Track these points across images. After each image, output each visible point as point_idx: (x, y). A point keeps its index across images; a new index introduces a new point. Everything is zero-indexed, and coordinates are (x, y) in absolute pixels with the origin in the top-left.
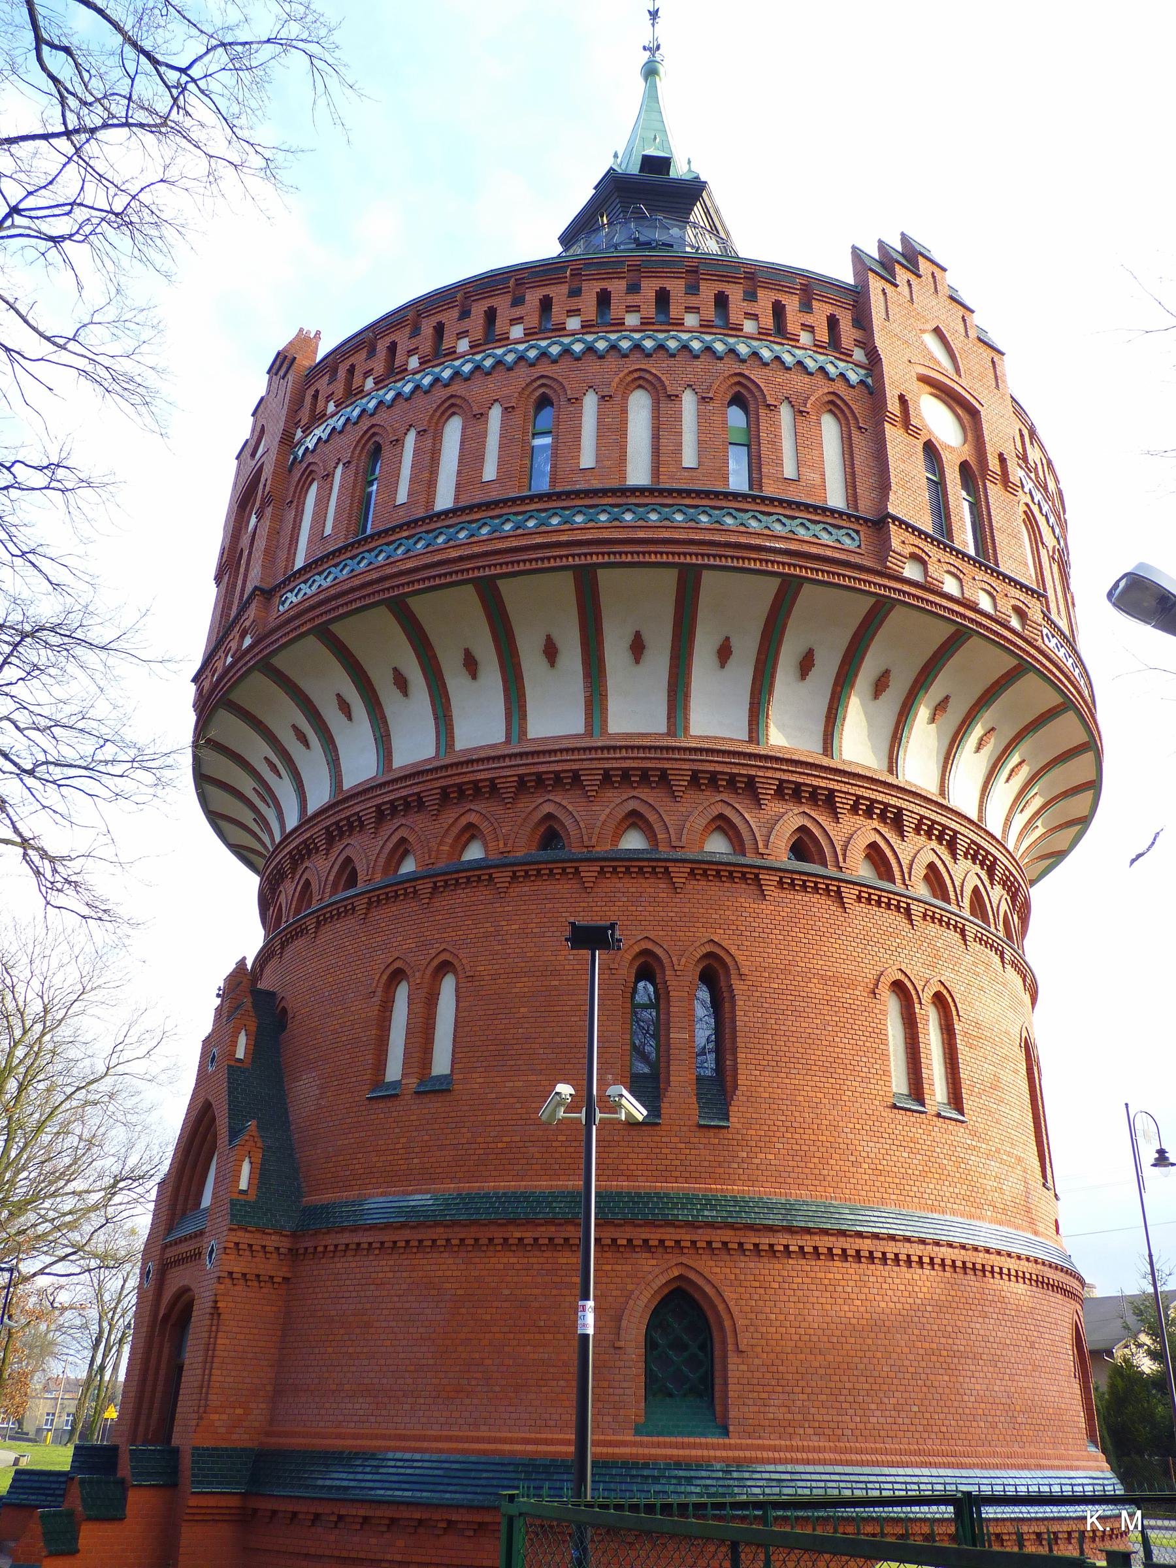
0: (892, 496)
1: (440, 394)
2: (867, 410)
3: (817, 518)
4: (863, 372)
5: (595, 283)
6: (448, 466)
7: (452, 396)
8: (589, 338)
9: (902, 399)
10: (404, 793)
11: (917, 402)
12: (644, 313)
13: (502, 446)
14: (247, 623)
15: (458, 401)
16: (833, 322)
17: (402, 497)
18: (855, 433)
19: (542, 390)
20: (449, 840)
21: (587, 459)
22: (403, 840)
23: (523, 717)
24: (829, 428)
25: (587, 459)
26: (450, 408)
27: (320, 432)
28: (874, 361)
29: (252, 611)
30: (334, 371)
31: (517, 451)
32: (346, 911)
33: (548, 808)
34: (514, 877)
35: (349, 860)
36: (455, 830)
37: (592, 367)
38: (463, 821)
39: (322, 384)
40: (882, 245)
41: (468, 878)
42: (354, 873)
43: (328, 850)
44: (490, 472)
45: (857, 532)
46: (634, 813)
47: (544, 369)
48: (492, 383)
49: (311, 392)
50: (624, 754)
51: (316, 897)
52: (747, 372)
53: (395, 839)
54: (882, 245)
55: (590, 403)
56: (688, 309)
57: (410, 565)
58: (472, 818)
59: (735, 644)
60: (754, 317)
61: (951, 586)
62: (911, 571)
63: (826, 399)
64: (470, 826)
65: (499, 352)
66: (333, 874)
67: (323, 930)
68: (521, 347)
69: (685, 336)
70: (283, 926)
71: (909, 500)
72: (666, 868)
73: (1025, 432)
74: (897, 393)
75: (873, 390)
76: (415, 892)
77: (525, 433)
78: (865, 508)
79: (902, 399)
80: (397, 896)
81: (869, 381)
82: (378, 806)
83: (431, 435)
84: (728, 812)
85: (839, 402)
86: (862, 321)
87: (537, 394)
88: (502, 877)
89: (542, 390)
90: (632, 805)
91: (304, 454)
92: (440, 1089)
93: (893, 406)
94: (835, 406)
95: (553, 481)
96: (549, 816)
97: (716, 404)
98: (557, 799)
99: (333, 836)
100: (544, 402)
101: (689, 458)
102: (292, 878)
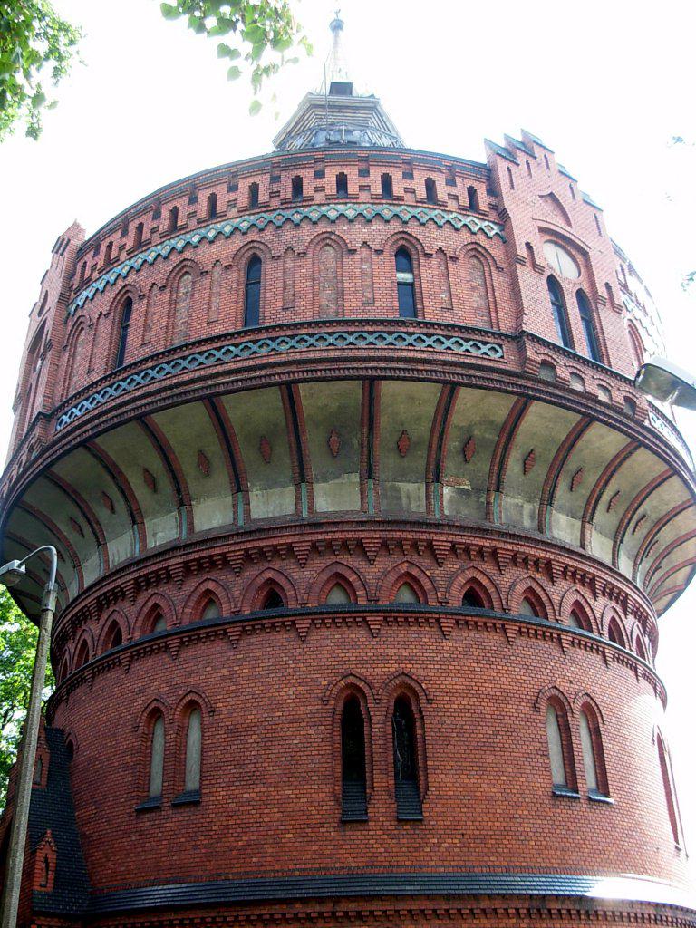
1: (175, 259)
3: (468, 336)
7: (184, 260)
9: (528, 244)
10: (154, 568)
12: (328, 192)
14: (33, 441)
15: (189, 263)
16: (472, 193)
20: (191, 604)
22: (156, 606)
27: (88, 293)
29: (37, 431)
30: (98, 246)
32: (114, 664)
33: (269, 575)
34: (244, 631)
35: (115, 624)
36: (195, 597)
38: (203, 588)
39: (89, 257)
40: (507, 138)
41: (207, 633)
42: (119, 633)
43: (99, 616)
45: (500, 346)
48: (214, 249)
49: (81, 264)
51: (91, 654)
52: (409, 231)
53: (150, 604)
54: (507, 138)
58: (211, 585)
64: (208, 592)
66: (104, 634)
67: (96, 680)
70: (68, 676)
72: (364, 618)
73: (625, 267)
74: (524, 241)
76: (166, 646)
78: (506, 326)
79: (528, 244)
80: (152, 651)
82: (136, 579)
85: (480, 249)
86: (493, 191)
88: (233, 632)
91: (76, 310)
92: (192, 802)
96: (271, 581)
98: (276, 567)
99: (101, 605)
102: (74, 639)
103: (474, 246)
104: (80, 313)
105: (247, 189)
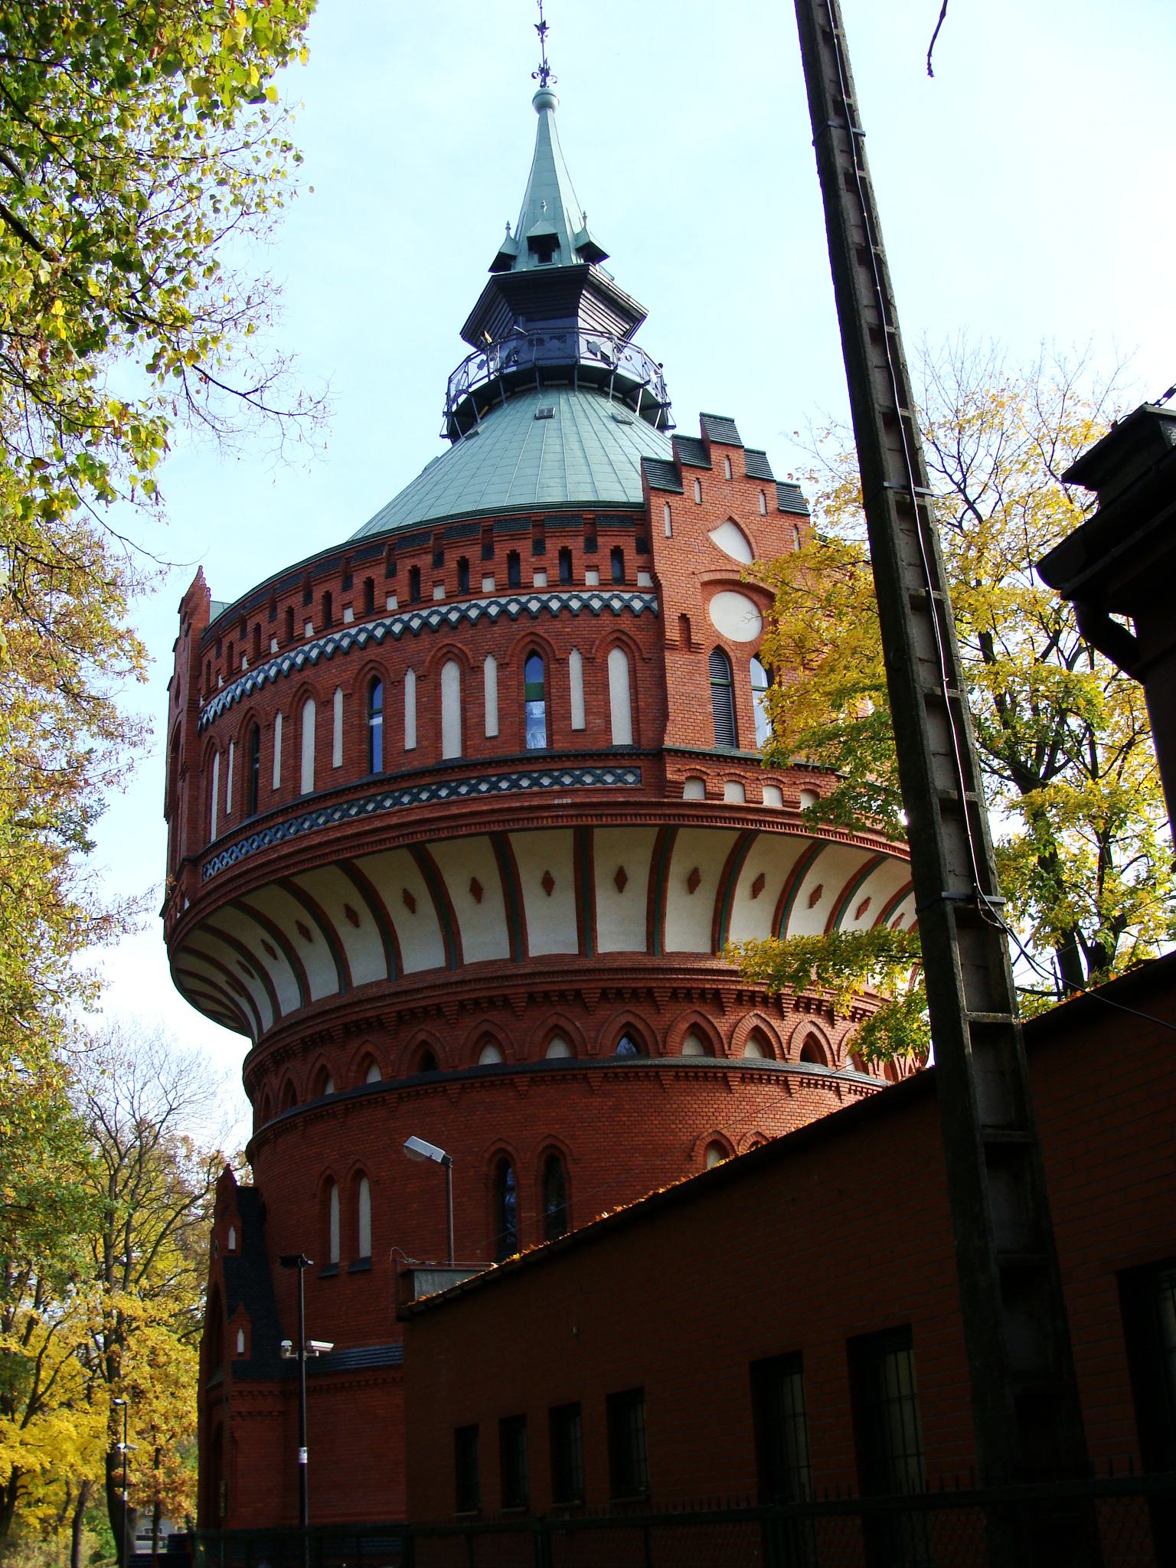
0: (670, 727)
2: (650, 639)
4: (647, 597)
5: (407, 561)
6: (311, 749)
8: (406, 617)
9: (684, 618)
11: (705, 613)
13: (345, 733)
17: (277, 784)
18: (640, 665)
19: (373, 672)
20: (354, 1068)
21: (410, 743)
22: (323, 1067)
23: (399, 956)
24: (617, 665)
25: (410, 743)
26: (304, 694)
28: (656, 588)
30: (219, 642)
31: (359, 735)
33: (422, 1036)
37: (412, 646)
38: (363, 1051)
44: (338, 761)
46: (486, 1033)
47: (373, 653)
50: (473, 986)
53: (318, 1065)
55: (410, 681)
56: (485, 575)
57: (286, 851)
58: (369, 1048)
59: (554, 874)
60: (543, 570)
61: (733, 795)
62: (692, 793)
63: (612, 637)
64: (368, 1054)
65: (337, 636)
68: (353, 631)
69: (483, 603)
71: (690, 727)
74: (676, 615)
75: (655, 617)
77: (361, 718)
78: (647, 743)
79: (684, 618)
81: (655, 605)
83: (294, 722)
84: (562, 1022)
85: (624, 638)
86: (645, 546)
87: (369, 677)
89: (373, 672)
90: (485, 1027)
93: (673, 633)
94: (620, 641)
95: (385, 767)
96: (424, 1042)
97: (513, 668)
100: (375, 683)
101: (491, 728)
103: (615, 635)
104: (211, 731)
105: (362, 586)
